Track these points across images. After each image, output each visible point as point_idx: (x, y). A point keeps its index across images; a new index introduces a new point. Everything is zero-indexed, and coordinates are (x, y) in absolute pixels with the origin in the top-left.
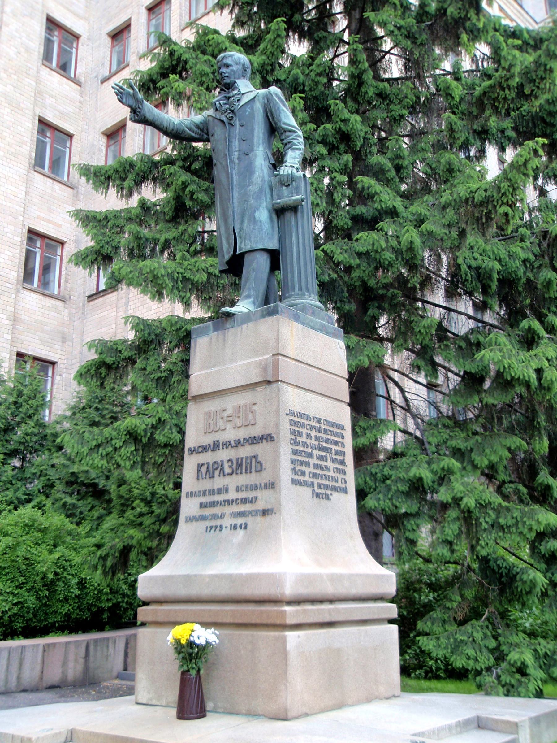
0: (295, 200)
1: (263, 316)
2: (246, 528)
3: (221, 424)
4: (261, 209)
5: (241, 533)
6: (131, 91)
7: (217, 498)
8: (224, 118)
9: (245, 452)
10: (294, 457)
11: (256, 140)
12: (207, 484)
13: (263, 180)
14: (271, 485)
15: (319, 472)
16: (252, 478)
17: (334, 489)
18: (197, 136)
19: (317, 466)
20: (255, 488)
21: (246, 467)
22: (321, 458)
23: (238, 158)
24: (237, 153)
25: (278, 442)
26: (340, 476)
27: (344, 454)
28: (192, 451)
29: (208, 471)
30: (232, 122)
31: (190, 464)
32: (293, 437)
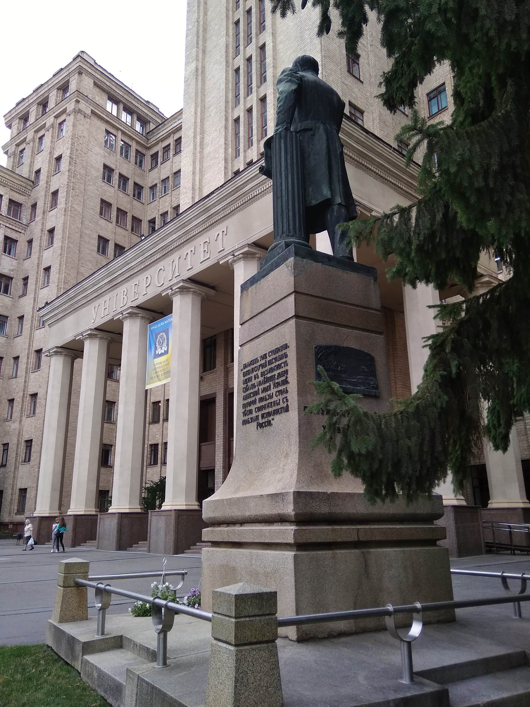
27: (286, 372)
32: (245, 386)
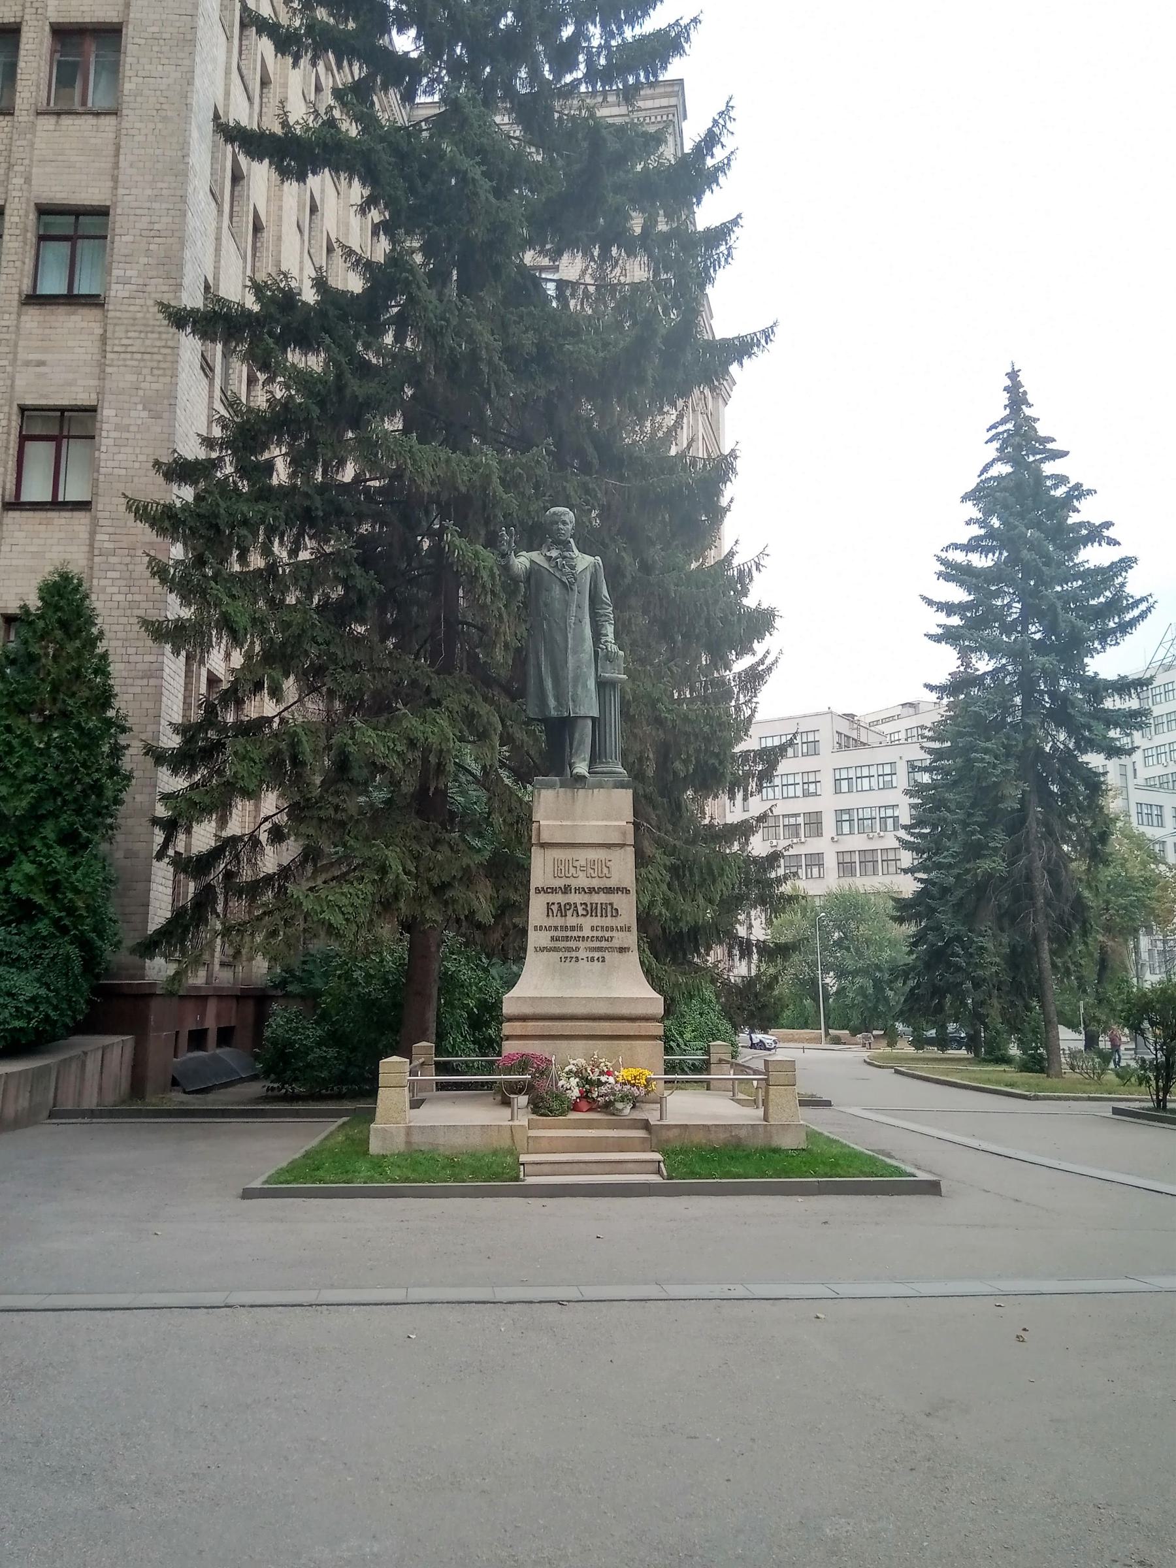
3: (572, 870)
7: (569, 934)
9: (600, 898)
12: (558, 921)
16: (609, 921)
20: (612, 929)
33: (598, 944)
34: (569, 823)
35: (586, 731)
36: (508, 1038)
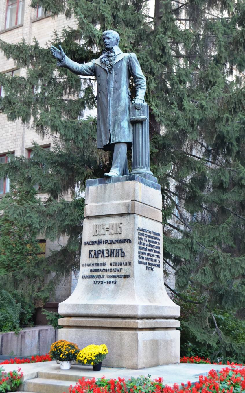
0: (142, 118)
1: (127, 180)
2: (115, 283)
4: (124, 120)
5: (112, 286)
6: (60, 51)
7: (100, 268)
8: (107, 69)
9: (116, 246)
10: (140, 250)
11: (122, 82)
12: (94, 261)
13: (126, 105)
14: (129, 264)
15: (149, 257)
16: (119, 260)
17: (155, 265)
18: (89, 74)
19: (149, 255)
20: (121, 264)
21: (116, 254)
22: (150, 251)
23: (113, 92)
24: (112, 89)
25: (133, 243)
26: (157, 259)
28: (86, 244)
29: (95, 254)
30: (111, 71)
31: (85, 250)
33: (113, 273)
34: (100, 204)
35: (122, 152)
36: (62, 327)
